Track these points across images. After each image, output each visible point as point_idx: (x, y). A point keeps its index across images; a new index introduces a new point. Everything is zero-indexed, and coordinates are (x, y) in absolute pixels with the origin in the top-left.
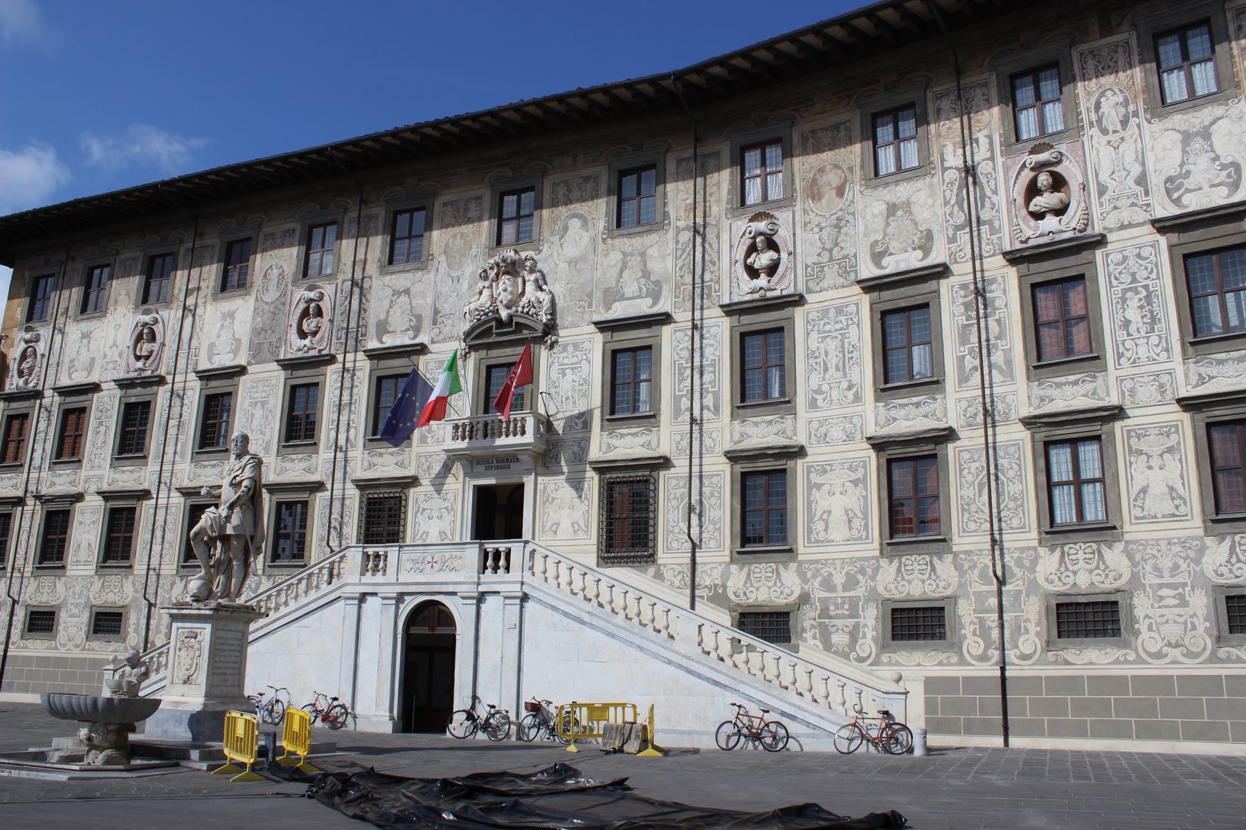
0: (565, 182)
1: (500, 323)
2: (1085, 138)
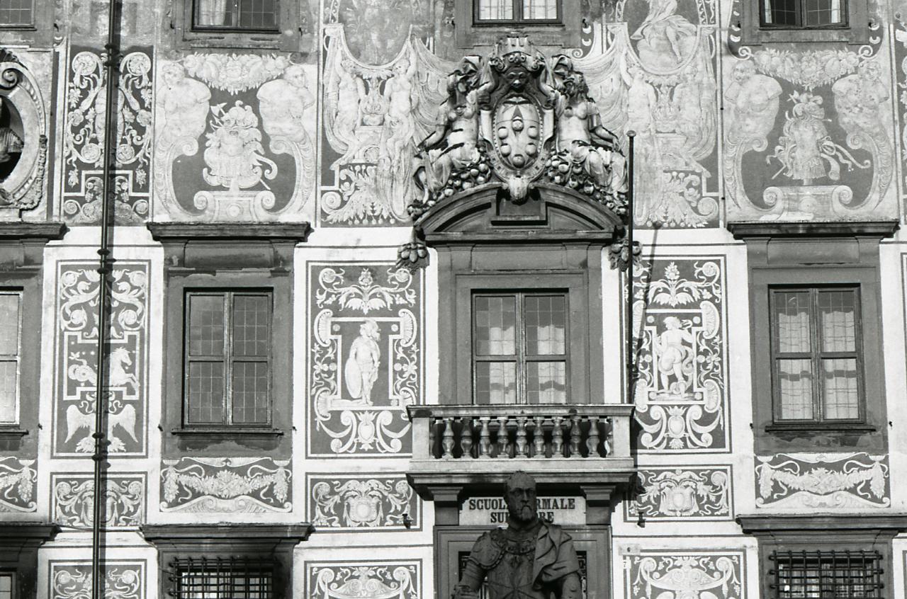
1: (503, 194)
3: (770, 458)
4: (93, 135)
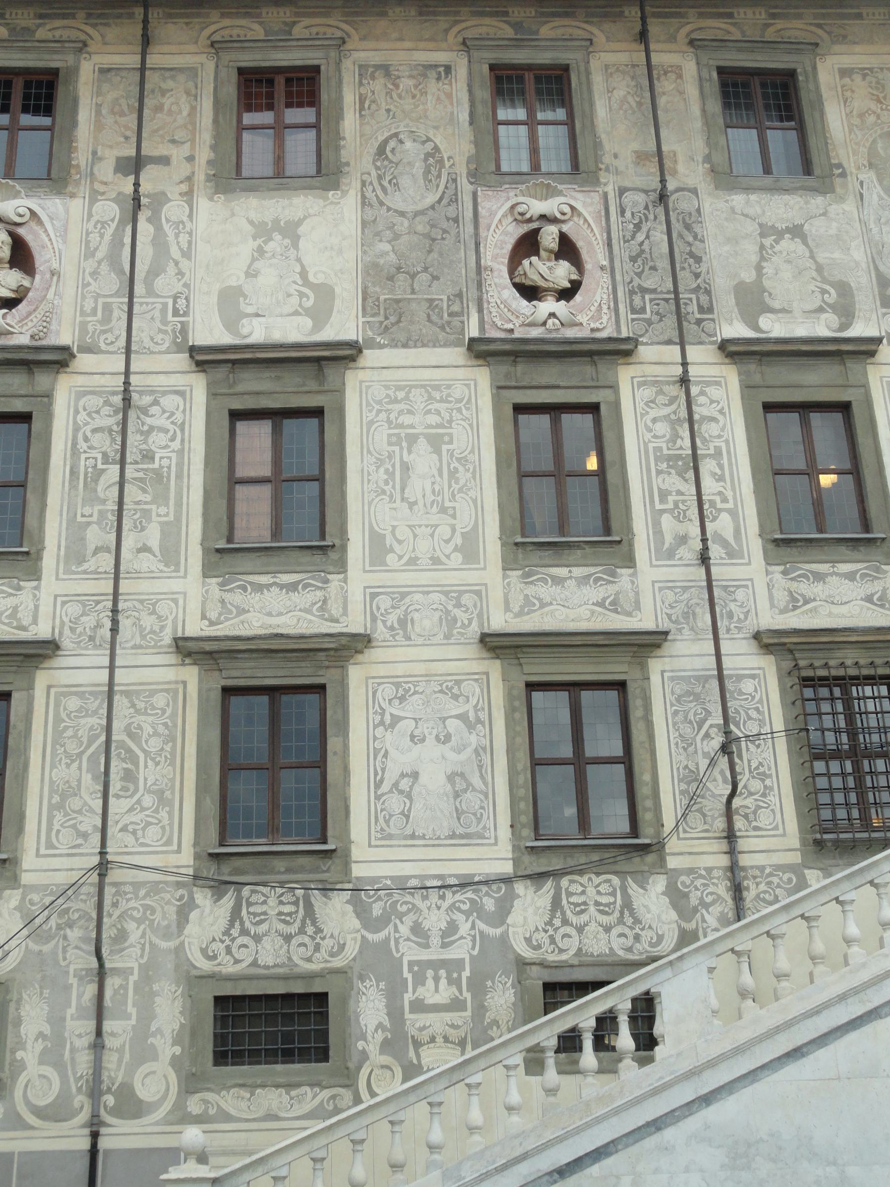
4: (651, 264)
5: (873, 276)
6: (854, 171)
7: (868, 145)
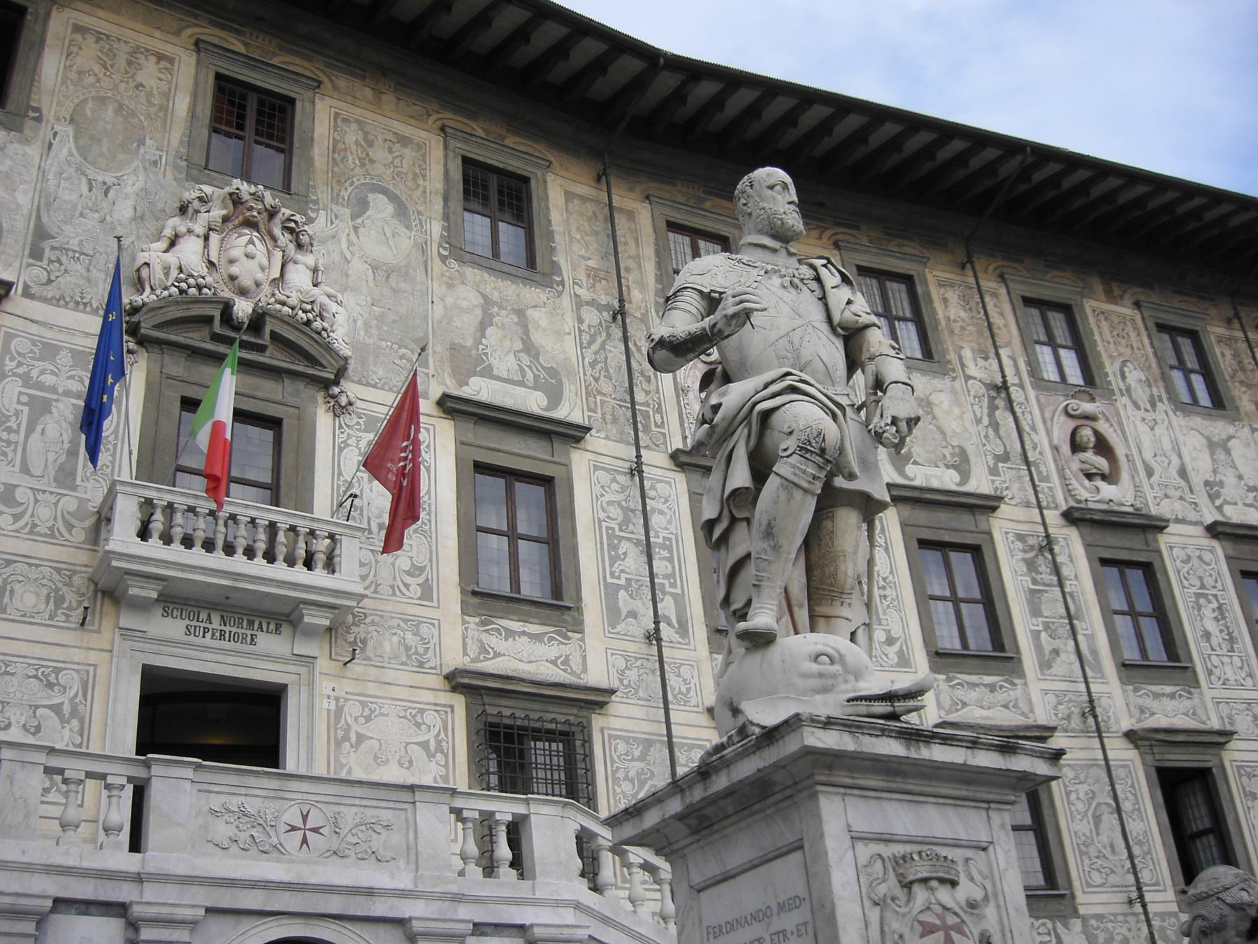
0: (357, 121)
2: (1118, 404)
3: (477, 620)
5: (32, 224)
6: (52, 119)
7: (77, 101)
